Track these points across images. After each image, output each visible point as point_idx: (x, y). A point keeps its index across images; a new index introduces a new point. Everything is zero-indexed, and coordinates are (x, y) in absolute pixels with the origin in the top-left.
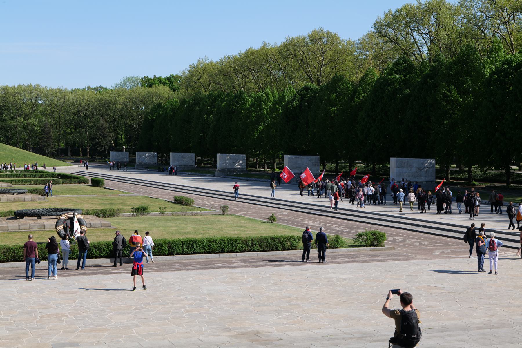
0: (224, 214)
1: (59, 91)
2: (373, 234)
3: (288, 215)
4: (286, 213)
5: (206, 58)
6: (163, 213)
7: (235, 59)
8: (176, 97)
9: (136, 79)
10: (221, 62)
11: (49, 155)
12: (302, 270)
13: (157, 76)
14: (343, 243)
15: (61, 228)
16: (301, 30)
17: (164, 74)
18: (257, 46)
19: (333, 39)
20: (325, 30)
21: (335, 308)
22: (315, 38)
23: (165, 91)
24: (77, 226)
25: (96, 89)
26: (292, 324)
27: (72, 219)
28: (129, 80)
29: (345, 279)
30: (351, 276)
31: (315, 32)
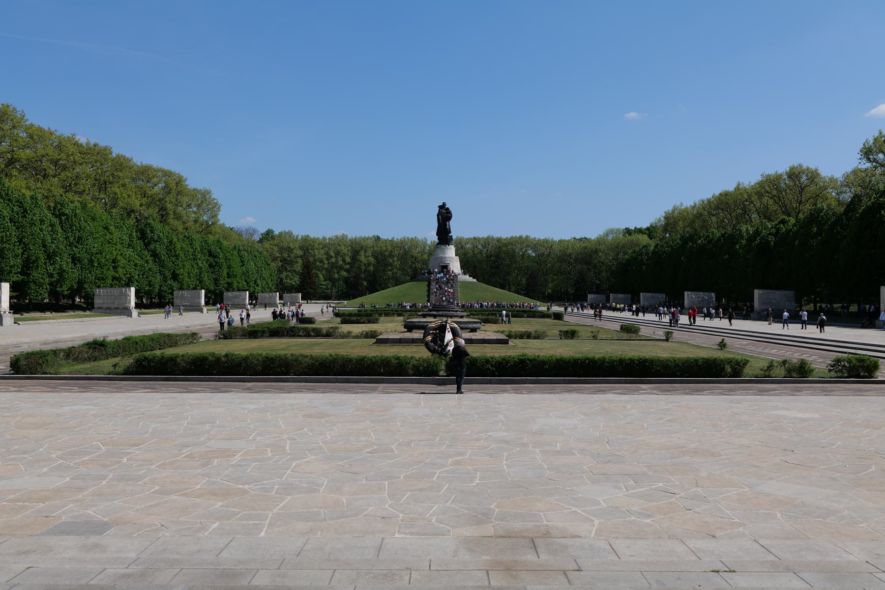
0: (667, 340)
1: (546, 241)
2: (861, 360)
3: (747, 345)
4: (745, 342)
5: (682, 204)
6: (595, 337)
7: (709, 201)
8: (652, 243)
9: (618, 230)
10: (693, 207)
11: (513, 289)
12: (731, 401)
13: (638, 227)
14: (812, 371)
15: (429, 338)
16: (779, 167)
17: (645, 225)
18: (731, 188)
19: (813, 176)
20: (805, 166)
21: (771, 479)
22: (794, 174)
23: (644, 239)
24: (449, 336)
25: (581, 240)
26: (649, 516)
27: (442, 329)
28: (611, 231)
29: (803, 420)
30: (817, 416)
31: (792, 169)
